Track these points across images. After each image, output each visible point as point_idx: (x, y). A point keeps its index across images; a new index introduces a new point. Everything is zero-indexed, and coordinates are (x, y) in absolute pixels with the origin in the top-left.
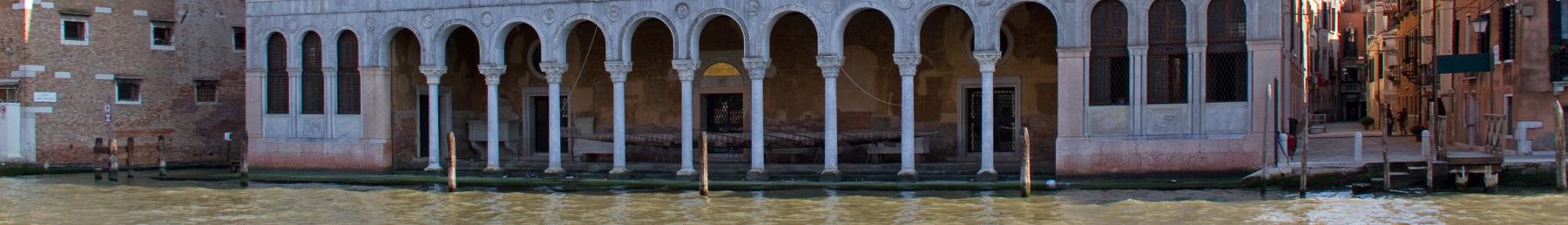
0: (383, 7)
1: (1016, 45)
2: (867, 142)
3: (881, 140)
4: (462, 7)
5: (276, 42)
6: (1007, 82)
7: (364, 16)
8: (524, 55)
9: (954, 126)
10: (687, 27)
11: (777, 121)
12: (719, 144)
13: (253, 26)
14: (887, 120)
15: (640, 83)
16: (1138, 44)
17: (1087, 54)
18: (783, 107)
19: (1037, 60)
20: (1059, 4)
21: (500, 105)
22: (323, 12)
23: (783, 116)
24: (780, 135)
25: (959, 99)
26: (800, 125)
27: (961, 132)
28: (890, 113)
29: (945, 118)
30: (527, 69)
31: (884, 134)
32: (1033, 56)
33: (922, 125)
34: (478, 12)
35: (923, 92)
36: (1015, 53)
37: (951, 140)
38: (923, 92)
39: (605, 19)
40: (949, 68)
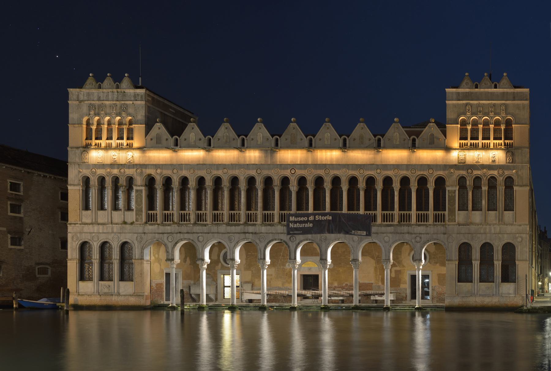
0: (146, 231)
1: (430, 259)
2: (371, 295)
3: (377, 294)
4: (188, 233)
6: (426, 273)
7: (136, 235)
8: (219, 256)
9: (406, 289)
10: (295, 246)
11: (333, 286)
12: (308, 295)
13: (72, 238)
14: (379, 286)
15: (273, 269)
16: (476, 260)
17: (457, 263)
18: (336, 280)
19: (438, 265)
20: (446, 243)
21: (207, 278)
22: (113, 232)
23: (336, 284)
24: (334, 292)
25: (408, 279)
26: (343, 288)
27: (409, 292)
28: (380, 284)
29: (402, 286)
30: (220, 262)
31: (377, 292)
32: (436, 263)
33: (393, 288)
34: (195, 235)
35: (393, 275)
36: (429, 262)
37: (404, 295)
38: (393, 275)
39: (258, 241)
40: (404, 266)
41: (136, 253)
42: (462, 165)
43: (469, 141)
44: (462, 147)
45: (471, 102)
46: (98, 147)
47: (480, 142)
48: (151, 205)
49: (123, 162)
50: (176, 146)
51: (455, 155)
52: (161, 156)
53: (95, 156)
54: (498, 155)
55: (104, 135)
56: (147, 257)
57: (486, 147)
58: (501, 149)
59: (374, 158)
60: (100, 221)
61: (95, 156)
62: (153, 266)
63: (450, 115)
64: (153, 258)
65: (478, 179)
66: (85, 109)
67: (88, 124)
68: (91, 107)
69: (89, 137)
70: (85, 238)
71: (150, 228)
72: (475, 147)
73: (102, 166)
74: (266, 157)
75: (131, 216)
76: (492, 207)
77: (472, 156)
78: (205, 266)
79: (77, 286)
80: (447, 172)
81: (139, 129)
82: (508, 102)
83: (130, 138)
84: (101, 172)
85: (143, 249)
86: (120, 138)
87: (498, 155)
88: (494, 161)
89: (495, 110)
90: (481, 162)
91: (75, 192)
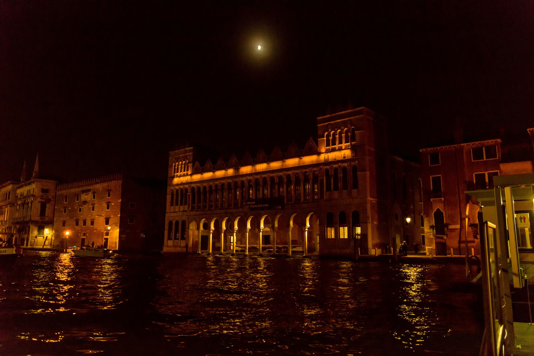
5: (171, 223)
41: (187, 224)
42: (327, 163)
43: (330, 147)
44: (327, 151)
45: (331, 122)
46: (177, 176)
47: (337, 146)
48: (193, 202)
49: (184, 182)
50: (202, 172)
51: (323, 157)
52: (197, 177)
53: (176, 180)
54: (347, 153)
55: (179, 171)
56: (191, 227)
57: (340, 149)
58: (348, 149)
59: (282, 165)
60: (176, 211)
61: (176, 180)
62: (194, 232)
63: (320, 132)
64: (194, 228)
65: (336, 170)
66: (174, 159)
67: (175, 166)
68: (176, 158)
69: (175, 173)
70: (171, 219)
71: (192, 213)
72: (334, 150)
73: (177, 185)
74: (236, 172)
75: (186, 208)
76: (345, 188)
77: (332, 156)
78: (212, 232)
79: (167, 242)
80: (318, 168)
81: (190, 165)
82: (352, 118)
83: (188, 170)
84: (177, 187)
85: (189, 224)
86: (184, 171)
87: (347, 153)
88: (344, 157)
89: (345, 124)
90: (337, 159)
91: (169, 197)
